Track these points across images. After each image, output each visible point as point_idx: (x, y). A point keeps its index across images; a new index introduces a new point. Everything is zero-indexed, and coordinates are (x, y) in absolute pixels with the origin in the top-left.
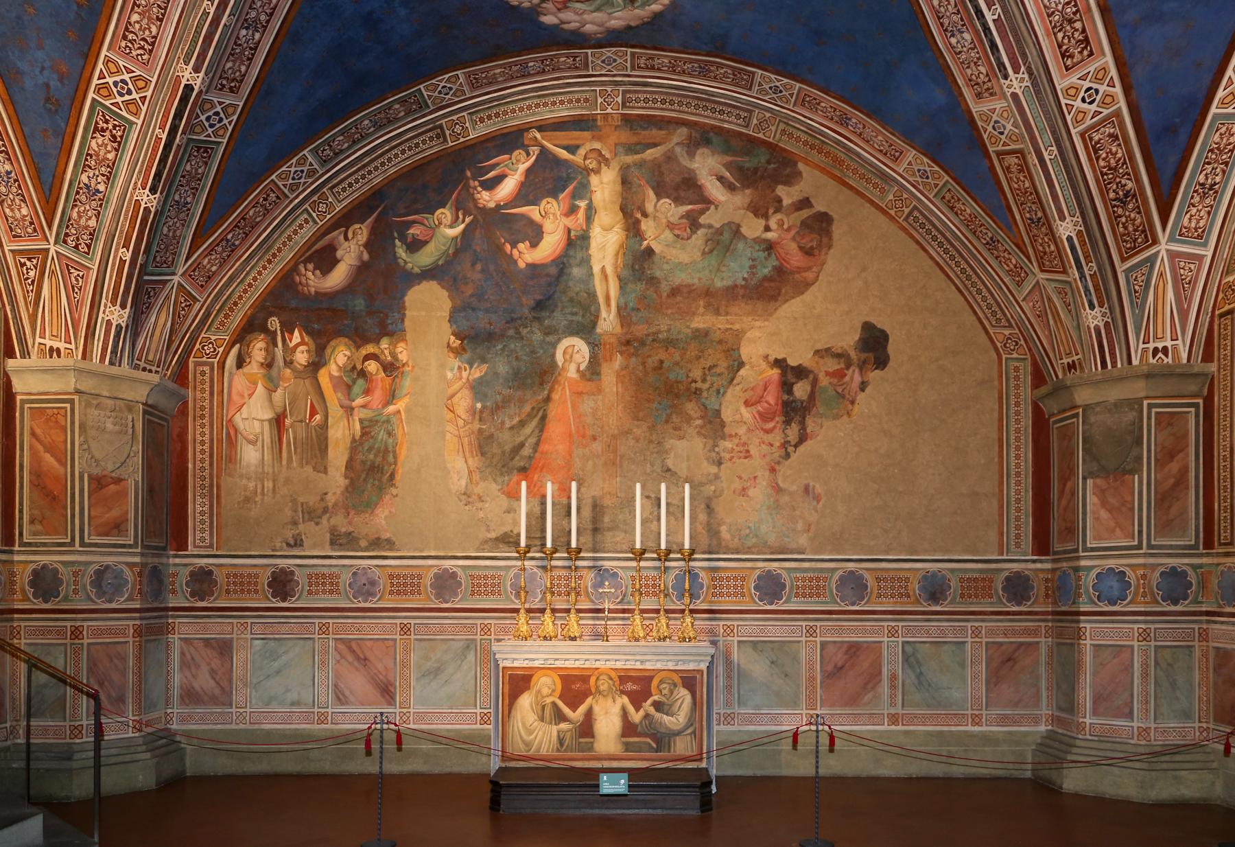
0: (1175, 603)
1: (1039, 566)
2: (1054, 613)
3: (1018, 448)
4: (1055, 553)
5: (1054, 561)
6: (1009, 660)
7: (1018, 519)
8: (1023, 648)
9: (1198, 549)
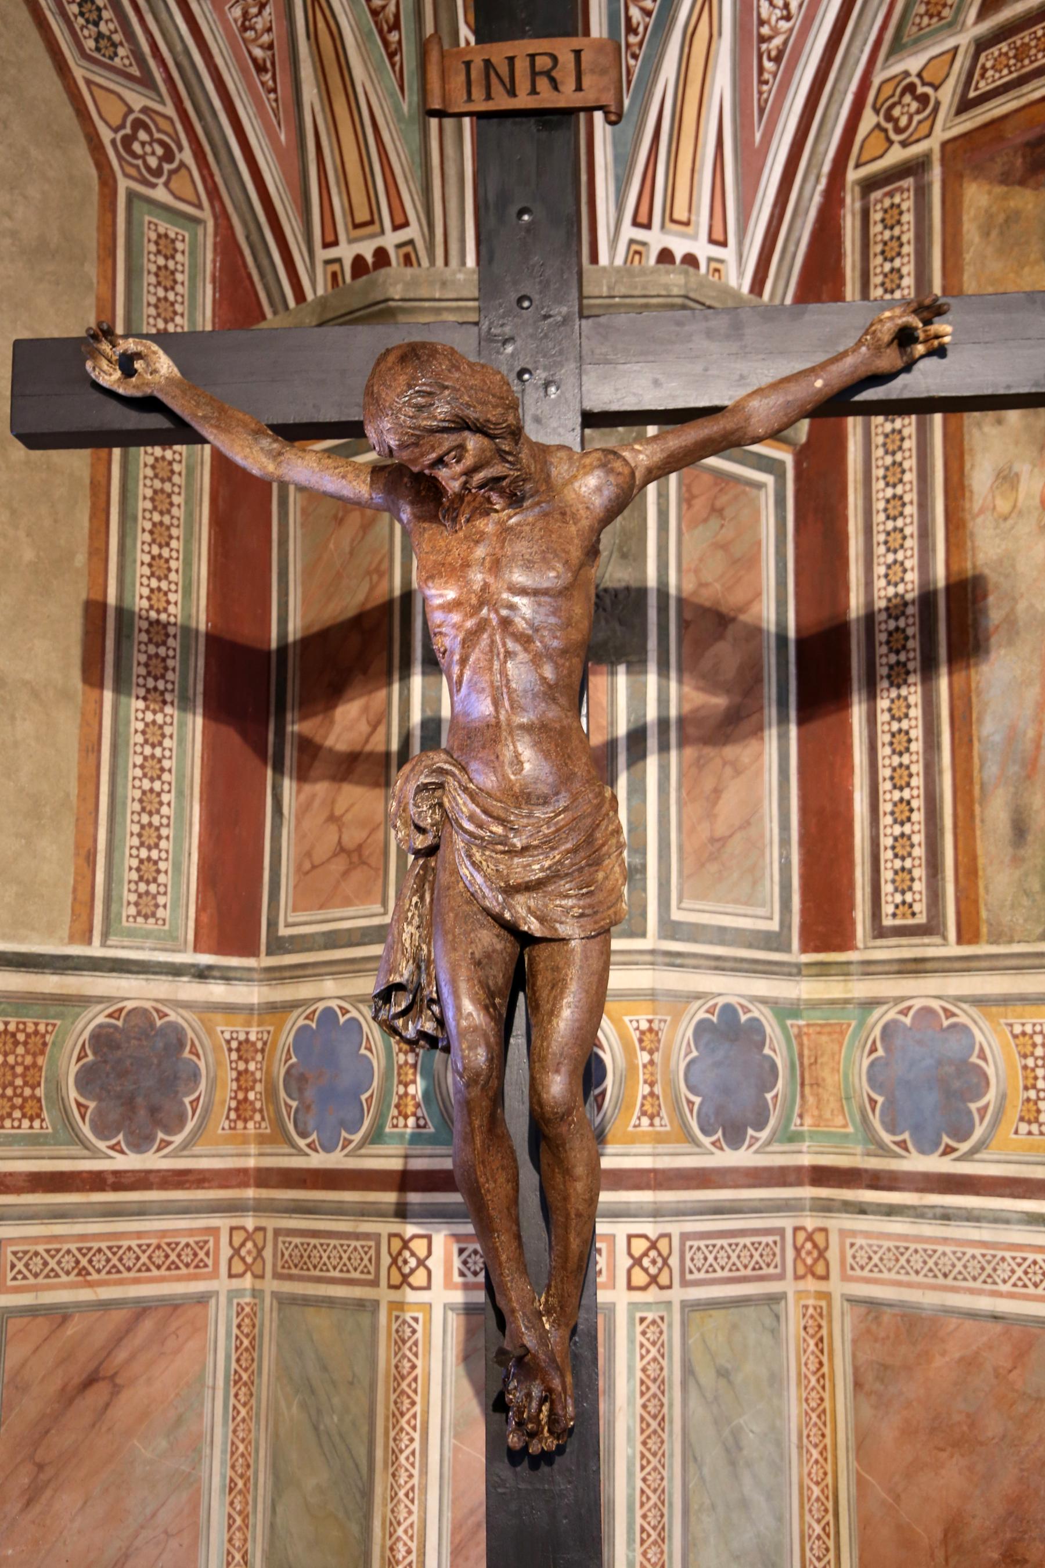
0: (735, 1137)
1: (217, 991)
2: (264, 1178)
3: (160, 535)
4: (278, 945)
5: (275, 975)
6: (89, 1382)
7: (150, 802)
8: (148, 1325)
9: (788, 949)
